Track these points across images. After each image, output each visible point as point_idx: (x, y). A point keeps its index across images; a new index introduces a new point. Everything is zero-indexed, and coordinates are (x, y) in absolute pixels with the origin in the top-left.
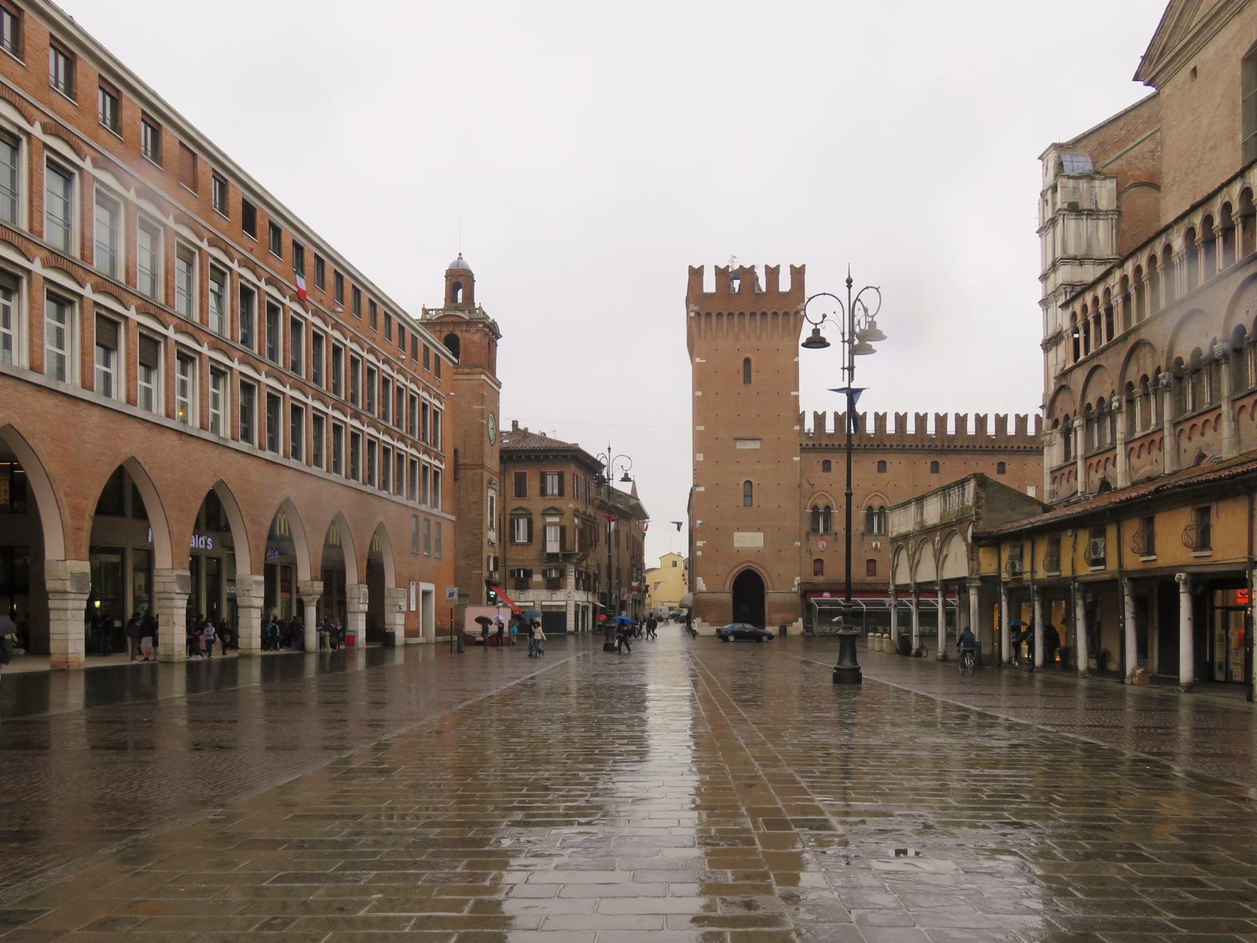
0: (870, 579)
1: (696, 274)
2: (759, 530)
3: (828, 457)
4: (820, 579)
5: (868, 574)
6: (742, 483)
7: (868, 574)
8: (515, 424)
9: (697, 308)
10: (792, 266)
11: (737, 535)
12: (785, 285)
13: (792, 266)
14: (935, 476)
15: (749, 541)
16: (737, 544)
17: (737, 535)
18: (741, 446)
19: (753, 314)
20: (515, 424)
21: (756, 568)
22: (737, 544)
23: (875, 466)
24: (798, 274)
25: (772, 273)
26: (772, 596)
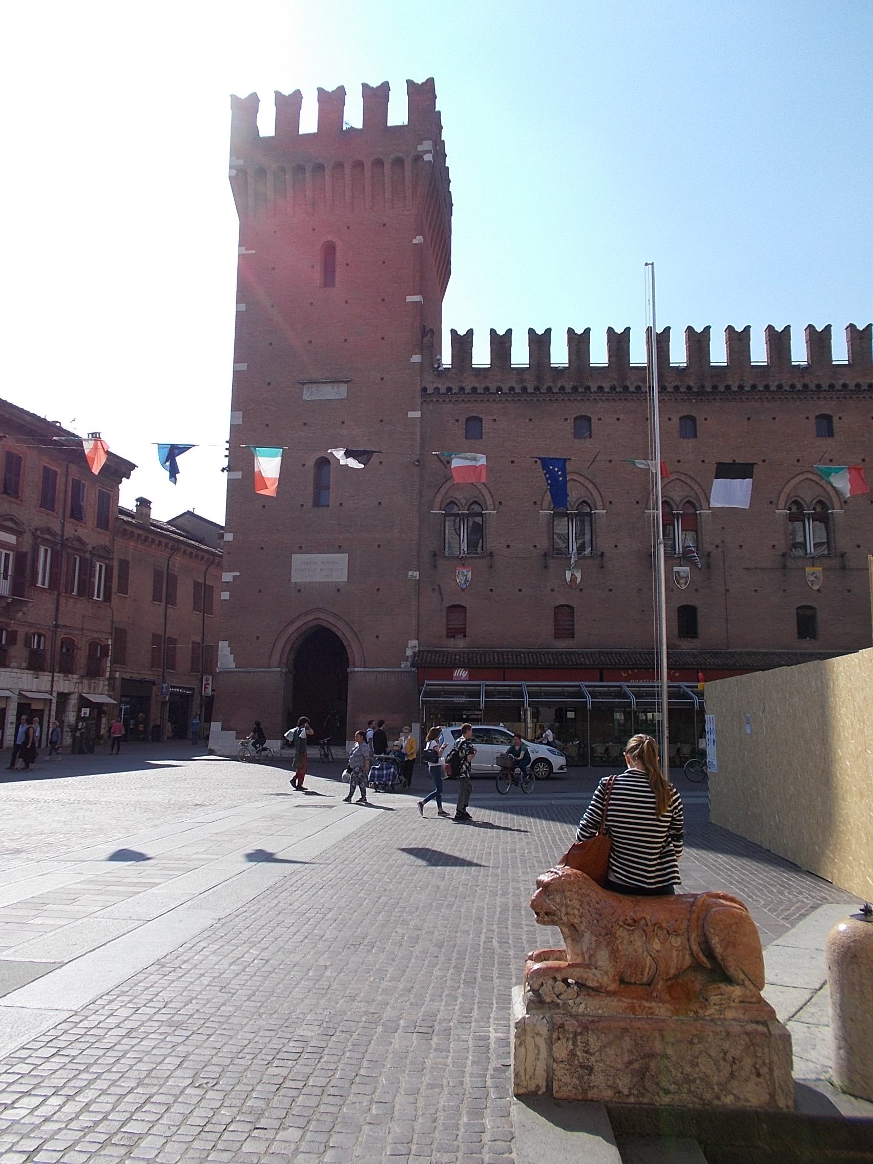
0: (563, 645)
1: (246, 108)
2: (340, 549)
3: (476, 409)
4: (460, 644)
5: (558, 635)
6: (311, 462)
7: (558, 635)
8: (144, 503)
9: (241, 162)
10: (410, 83)
11: (297, 559)
12: (398, 114)
13: (410, 83)
14: (690, 443)
15: (320, 569)
16: (296, 578)
17: (297, 559)
18: (310, 394)
19: (340, 165)
20: (144, 503)
21: (330, 621)
22: (296, 578)
23: (569, 426)
24: (423, 95)
25: (376, 98)
26: (362, 674)
